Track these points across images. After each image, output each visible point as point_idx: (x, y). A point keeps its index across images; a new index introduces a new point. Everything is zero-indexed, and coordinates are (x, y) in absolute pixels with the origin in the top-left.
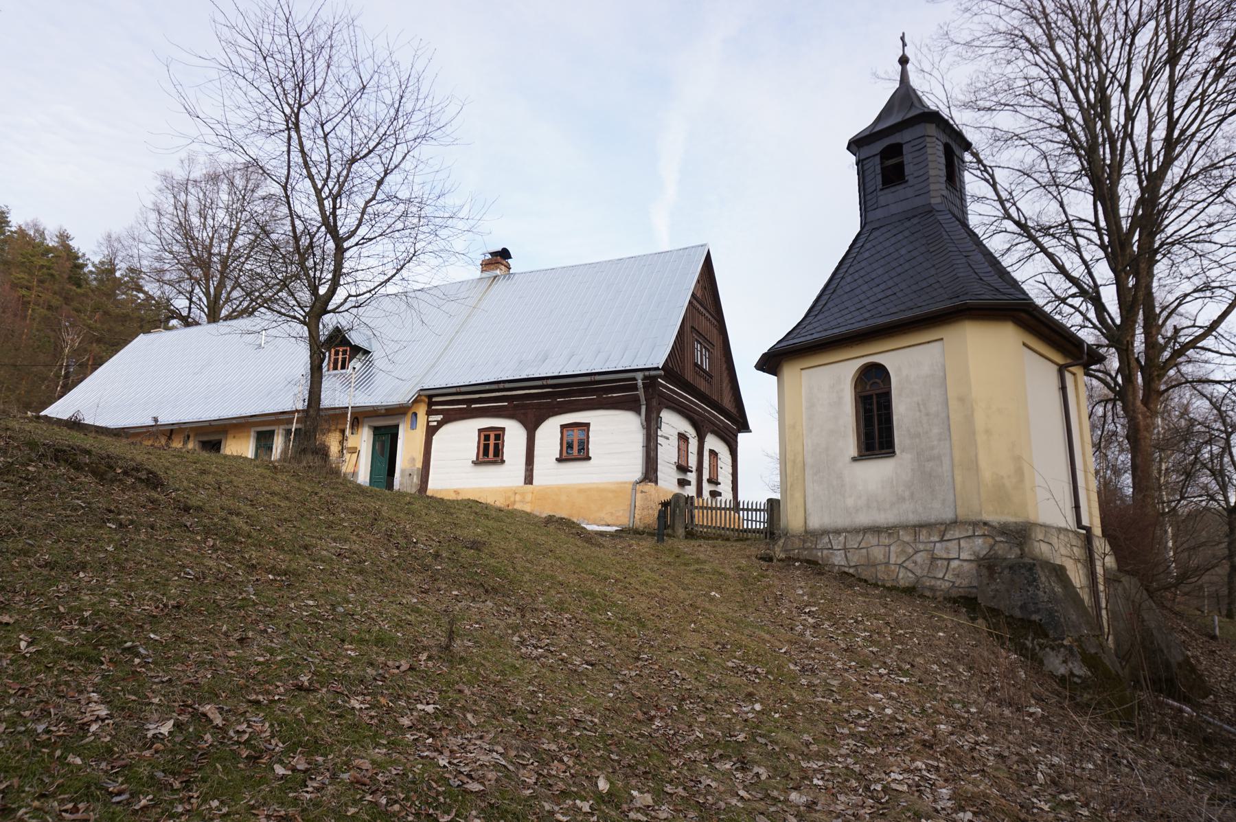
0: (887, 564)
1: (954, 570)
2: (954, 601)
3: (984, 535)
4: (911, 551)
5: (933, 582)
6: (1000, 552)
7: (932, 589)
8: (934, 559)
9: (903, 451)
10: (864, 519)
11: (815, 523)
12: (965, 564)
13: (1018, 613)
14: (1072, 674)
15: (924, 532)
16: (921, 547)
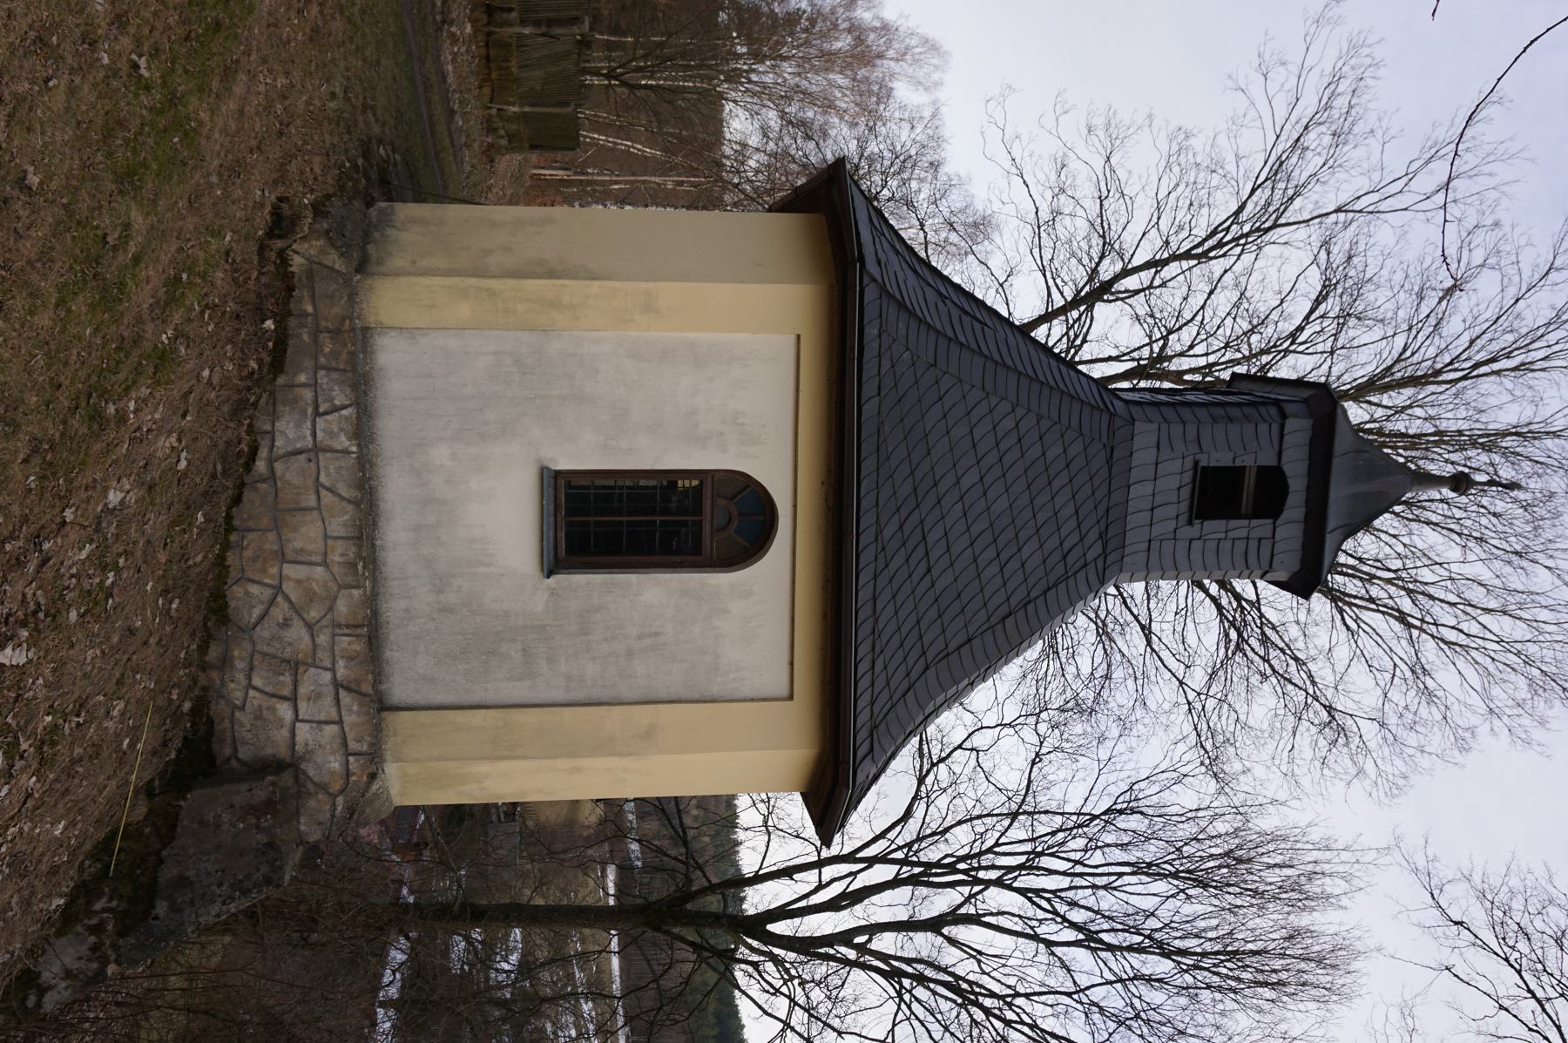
0: (282, 557)
1: (272, 709)
2: (201, 707)
3: (348, 774)
4: (314, 614)
5: (240, 665)
6: (312, 803)
7: (225, 662)
8: (295, 667)
9: (553, 593)
10: (395, 488)
11: (391, 354)
12: (285, 732)
13: (168, 873)
14: (43, 991)
15: (358, 647)
16: (323, 639)
